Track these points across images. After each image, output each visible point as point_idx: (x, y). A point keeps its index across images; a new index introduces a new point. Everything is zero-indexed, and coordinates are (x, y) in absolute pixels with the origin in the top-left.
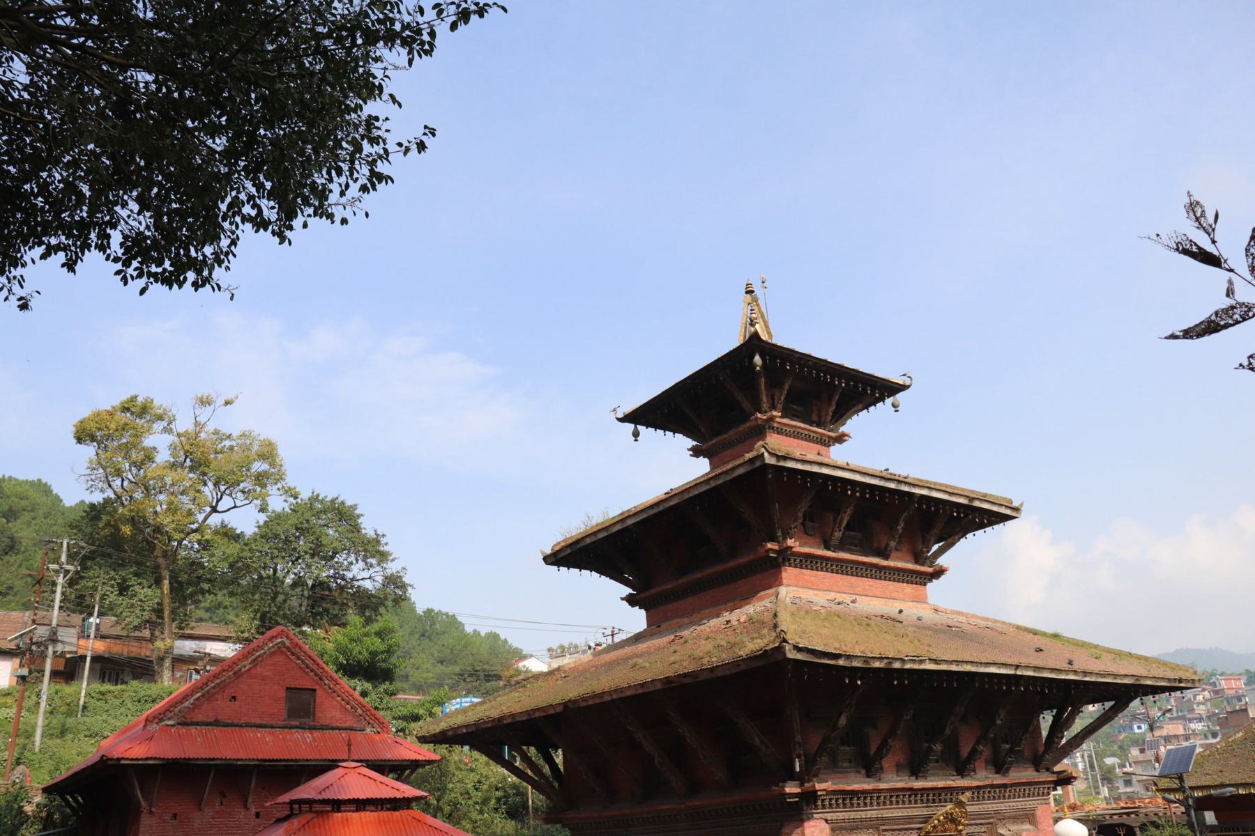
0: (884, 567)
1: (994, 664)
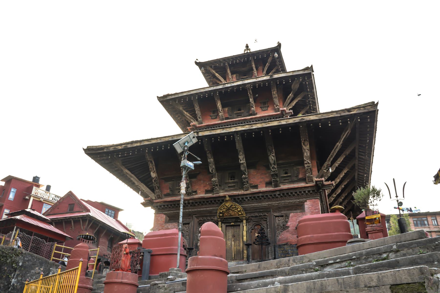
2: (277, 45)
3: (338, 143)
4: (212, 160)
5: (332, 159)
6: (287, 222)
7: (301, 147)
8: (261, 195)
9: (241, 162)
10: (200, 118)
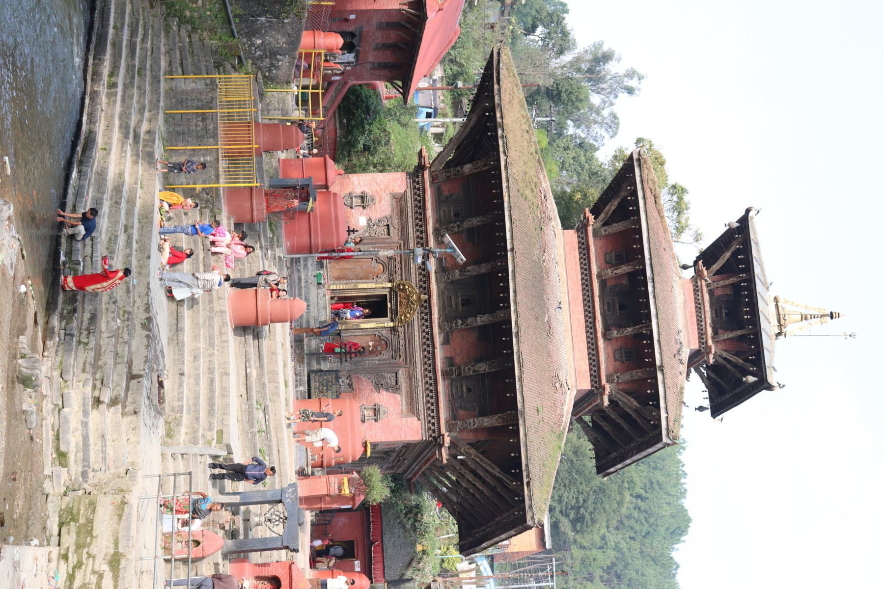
0: (596, 337)
1: (511, 223)
2: (769, 380)
3: (498, 469)
4: (484, 271)
5: (478, 460)
6: (387, 390)
7: (492, 413)
8: (430, 349)
9: (478, 318)
10: (605, 231)
